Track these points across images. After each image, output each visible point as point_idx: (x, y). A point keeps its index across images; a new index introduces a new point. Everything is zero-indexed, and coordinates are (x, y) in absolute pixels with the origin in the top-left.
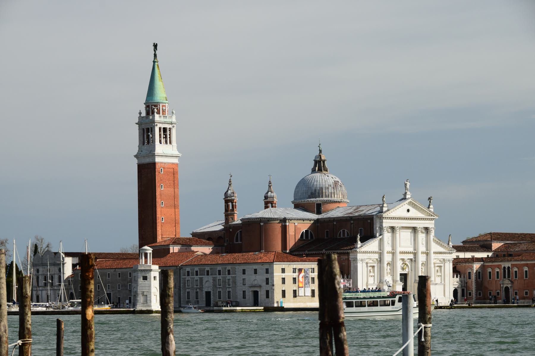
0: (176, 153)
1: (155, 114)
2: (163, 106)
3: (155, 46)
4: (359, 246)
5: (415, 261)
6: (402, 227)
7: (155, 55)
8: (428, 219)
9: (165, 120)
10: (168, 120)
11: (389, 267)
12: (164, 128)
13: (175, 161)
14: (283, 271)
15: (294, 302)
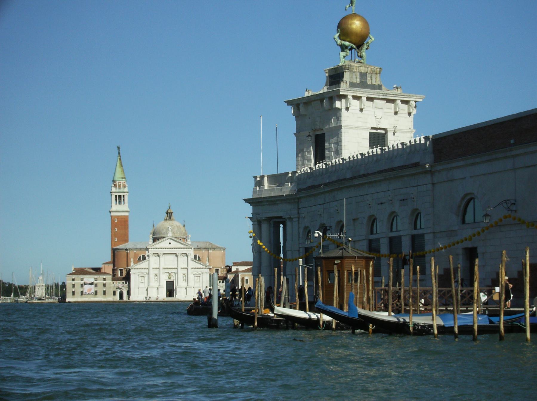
0: (128, 209)
1: (113, 187)
2: (119, 182)
3: (119, 148)
4: (132, 265)
5: (177, 274)
6: (164, 254)
7: (119, 153)
8: (185, 248)
9: (120, 191)
10: (122, 190)
11: (156, 277)
12: (119, 196)
13: (127, 214)
14: (73, 280)
15: (81, 298)
